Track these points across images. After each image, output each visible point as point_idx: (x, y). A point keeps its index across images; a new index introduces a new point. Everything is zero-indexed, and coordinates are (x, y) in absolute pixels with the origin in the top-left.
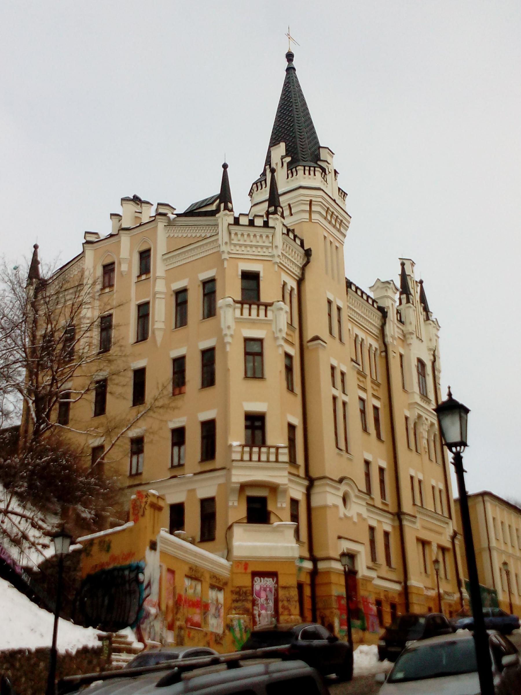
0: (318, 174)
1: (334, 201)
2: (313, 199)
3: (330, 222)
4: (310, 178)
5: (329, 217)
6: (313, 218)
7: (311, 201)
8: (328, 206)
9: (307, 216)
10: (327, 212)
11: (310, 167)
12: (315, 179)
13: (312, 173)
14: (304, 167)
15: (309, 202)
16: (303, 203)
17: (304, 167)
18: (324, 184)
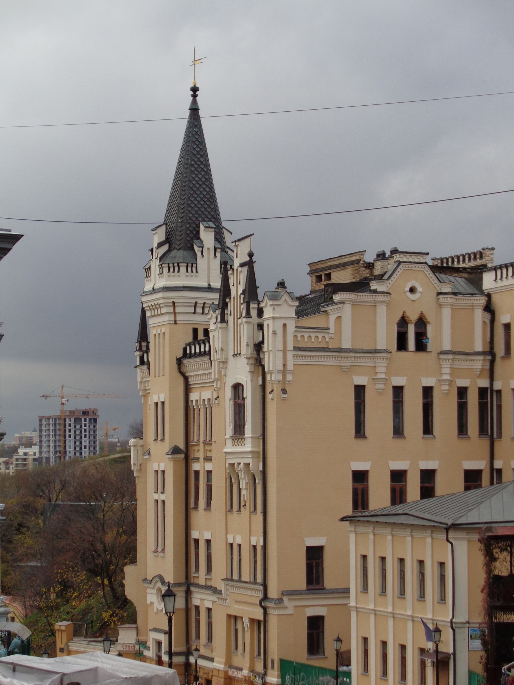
0: (183, 269)
1: (209, 289)
2: (176, 301)
3: (203, 313)
4: (174, 276)
5: (199, 310)
6: (177, 320)
7: (174, 303)
8: (194, 301)
9: (172, 318)
10: (195, 307)
11: (173, 264)
12: (179, 276)
13: (176, 269)
14: (169, 264)
15: (171, 304)
16: (166, 305)
17: (169, 264)
18: (192, 276)
